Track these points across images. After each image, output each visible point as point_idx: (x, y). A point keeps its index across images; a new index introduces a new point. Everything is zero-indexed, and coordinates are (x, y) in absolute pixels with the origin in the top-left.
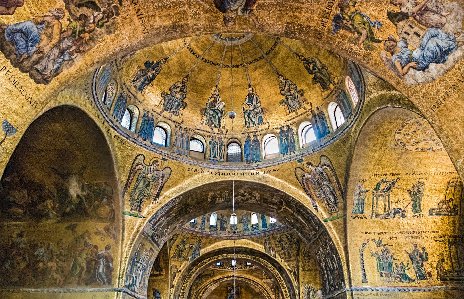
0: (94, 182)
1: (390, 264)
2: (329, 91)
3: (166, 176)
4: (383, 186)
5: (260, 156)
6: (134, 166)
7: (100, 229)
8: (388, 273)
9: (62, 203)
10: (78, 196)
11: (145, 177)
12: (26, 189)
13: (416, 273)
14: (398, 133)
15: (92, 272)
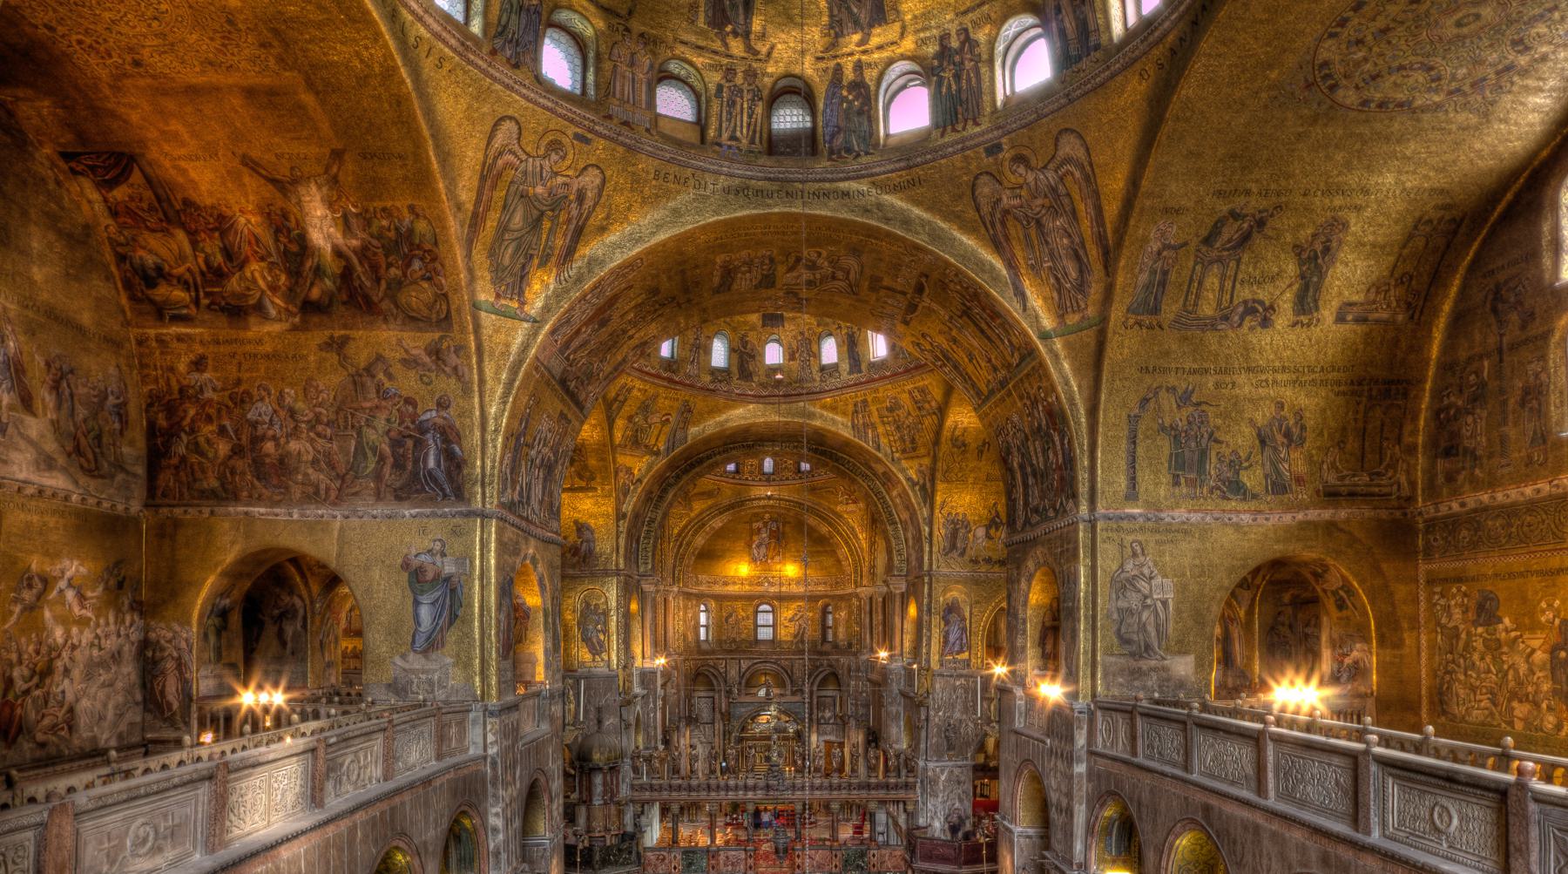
1: (1204, 454)
4: (1230, 232)
5: (871, 135)
7: (414, 352)
9: (295, 274)
10: (338, 253)
11: (527, 195)
12: (183, 226)
13: (1266, 477)
15: (410, 466)
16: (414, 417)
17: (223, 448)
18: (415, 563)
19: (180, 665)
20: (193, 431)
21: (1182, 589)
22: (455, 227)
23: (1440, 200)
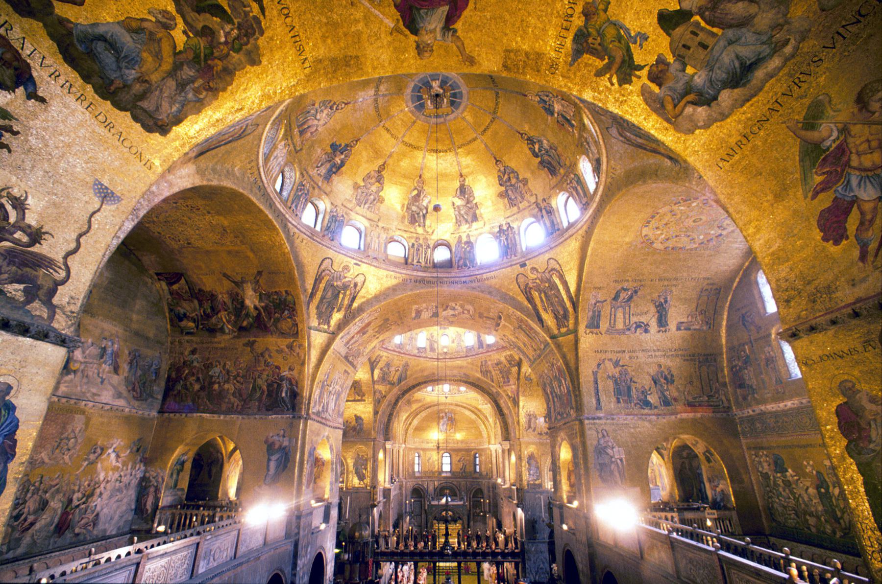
1: (629, 389)
2: (559, 178)
3: (359, 284)
4: (623, 296)
8: (626, 398)
10: (256, 308)
12: (197, 298)
18: (271, 441)
21: (628, 453)
22: (303, 298)
23: (709, 282)
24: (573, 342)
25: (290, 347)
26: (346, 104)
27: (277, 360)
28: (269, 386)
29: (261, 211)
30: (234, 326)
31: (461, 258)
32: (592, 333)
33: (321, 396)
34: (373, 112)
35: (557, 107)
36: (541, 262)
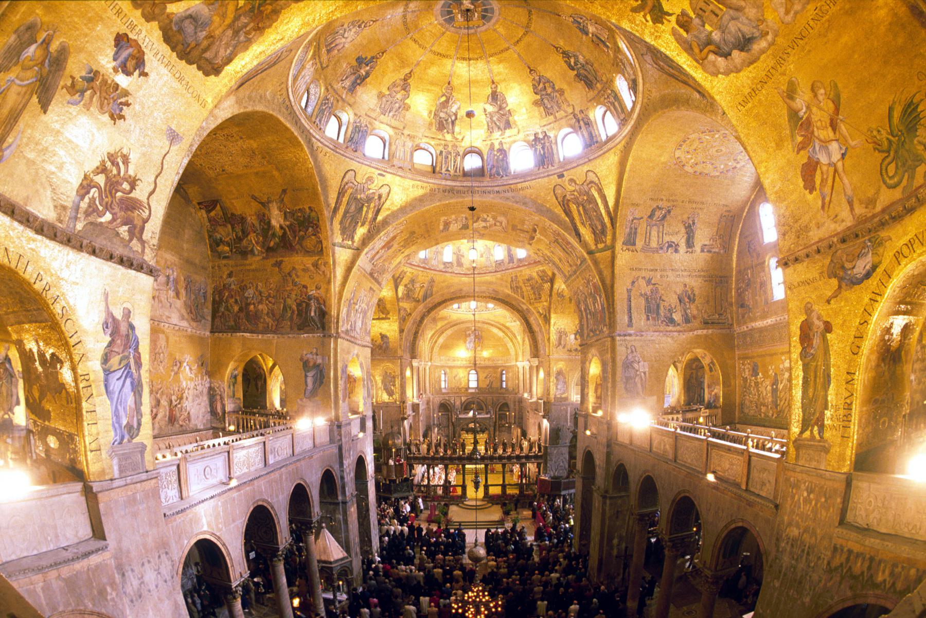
0: (298, 208)
1: (658, 306)
6: (343, 185)
8: (655, 316)
14: (679, 149)
16: (306, 293)
17: (236, 308)
19: (222, 398)
20: (227, 302)
21: (651, 367)
22: (327, 214)
24: (610, 259)
25: (316, 265)
26: (374, 21)
27: (304, 280)
28: (299, 305)
29: (287, 129)
30: (262, 247)
31: (493, 166)
32: (628, 249)
33: (348, 315)
34: (401, 27)
35: (591, 29)
36: (579, 174)
